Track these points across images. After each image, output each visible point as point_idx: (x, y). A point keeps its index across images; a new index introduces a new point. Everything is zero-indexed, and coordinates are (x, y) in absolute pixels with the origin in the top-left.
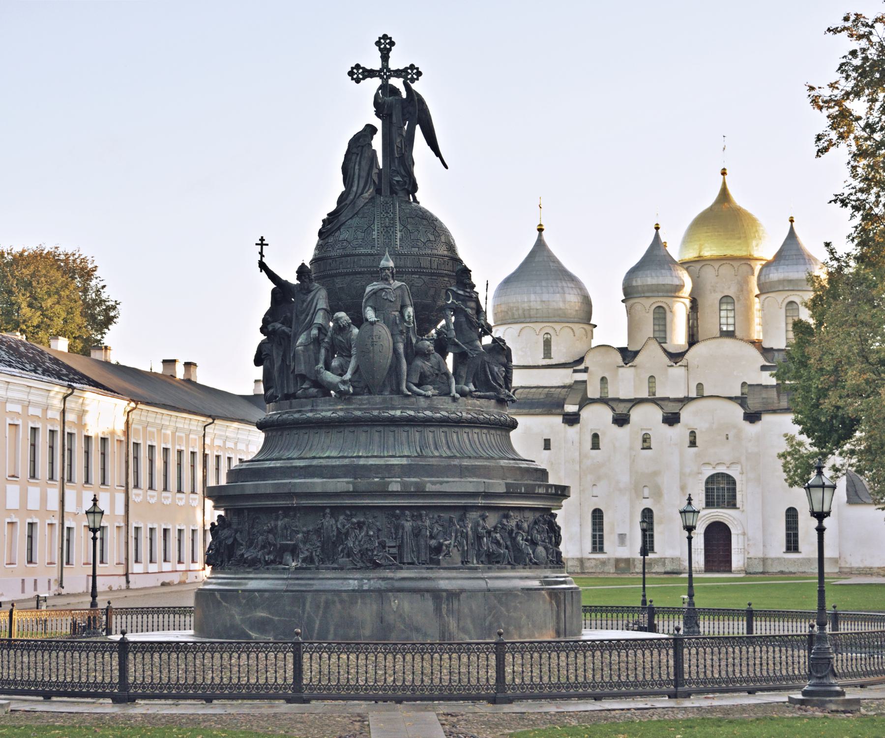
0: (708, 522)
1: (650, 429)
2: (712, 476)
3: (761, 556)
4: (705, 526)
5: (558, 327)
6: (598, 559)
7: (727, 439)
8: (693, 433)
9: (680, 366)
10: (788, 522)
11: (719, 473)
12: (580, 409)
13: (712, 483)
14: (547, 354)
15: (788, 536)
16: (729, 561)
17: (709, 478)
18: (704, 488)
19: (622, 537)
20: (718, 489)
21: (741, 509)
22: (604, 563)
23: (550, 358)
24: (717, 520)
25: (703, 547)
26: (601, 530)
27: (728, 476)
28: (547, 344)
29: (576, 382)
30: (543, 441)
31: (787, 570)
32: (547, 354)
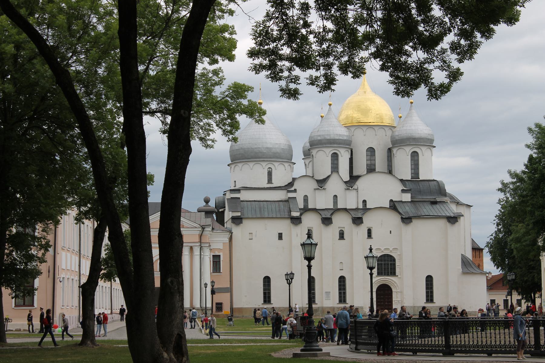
0: (379, 285)
1: (344, 227)
3: (412, 305)
4: (377, 287)
5: (276, 164)
7: (391, 233)
9: (354, 189)
10: (427, 285)
12: (301, 215)
13: (381, 261)
14: (270, 181)
15: (427, 293)
23: (272, 183)
24: (384, 283)
27: (391, 256)
28: (270, 174)
29: (289, 198)
32: (270, 181)
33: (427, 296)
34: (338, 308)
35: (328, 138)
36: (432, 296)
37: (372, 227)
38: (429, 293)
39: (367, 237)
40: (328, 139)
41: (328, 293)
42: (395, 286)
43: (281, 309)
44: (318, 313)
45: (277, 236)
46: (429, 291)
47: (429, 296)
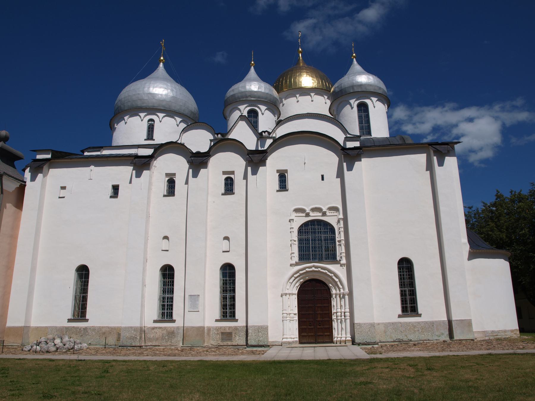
1: (233, 173)
2: (306, 224)
5: (161, 115)
6: (165, 327)
7: (323, 179)
8: (283, 177)
11: (313, 222)
15: (403, 294)
16: (330, 329)
17: (301, 226)
18: (296, 239)
19: (195, 298)
20: (314, 240)
21: (342, 262)
22: (171, 333)
25: (296, 311)
26: (172, 291)
28: (151, 129)
30: (111, 187)
31: (405, 339)
33: (403, 301)
34: (218, 329)
35: (243, 90)
36: (414, 301)
37: (286, 171)
38: (405, 295)
39: (277, 187)
40: (242, 92)
41: (195, 298)
42: (336, 282)
43: (104, 330)
44: (176, 339)
45: (110, 191)
46: (405, 291)
47: (406, 301)
